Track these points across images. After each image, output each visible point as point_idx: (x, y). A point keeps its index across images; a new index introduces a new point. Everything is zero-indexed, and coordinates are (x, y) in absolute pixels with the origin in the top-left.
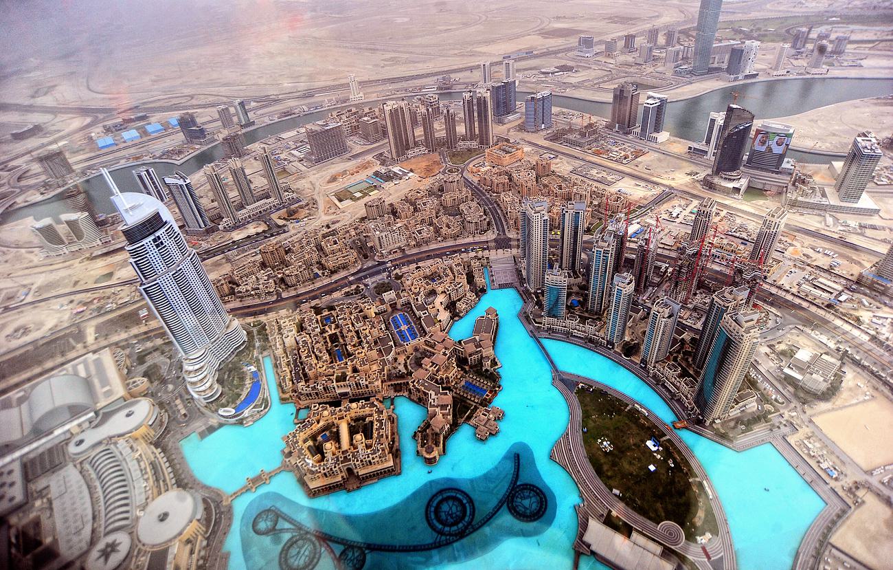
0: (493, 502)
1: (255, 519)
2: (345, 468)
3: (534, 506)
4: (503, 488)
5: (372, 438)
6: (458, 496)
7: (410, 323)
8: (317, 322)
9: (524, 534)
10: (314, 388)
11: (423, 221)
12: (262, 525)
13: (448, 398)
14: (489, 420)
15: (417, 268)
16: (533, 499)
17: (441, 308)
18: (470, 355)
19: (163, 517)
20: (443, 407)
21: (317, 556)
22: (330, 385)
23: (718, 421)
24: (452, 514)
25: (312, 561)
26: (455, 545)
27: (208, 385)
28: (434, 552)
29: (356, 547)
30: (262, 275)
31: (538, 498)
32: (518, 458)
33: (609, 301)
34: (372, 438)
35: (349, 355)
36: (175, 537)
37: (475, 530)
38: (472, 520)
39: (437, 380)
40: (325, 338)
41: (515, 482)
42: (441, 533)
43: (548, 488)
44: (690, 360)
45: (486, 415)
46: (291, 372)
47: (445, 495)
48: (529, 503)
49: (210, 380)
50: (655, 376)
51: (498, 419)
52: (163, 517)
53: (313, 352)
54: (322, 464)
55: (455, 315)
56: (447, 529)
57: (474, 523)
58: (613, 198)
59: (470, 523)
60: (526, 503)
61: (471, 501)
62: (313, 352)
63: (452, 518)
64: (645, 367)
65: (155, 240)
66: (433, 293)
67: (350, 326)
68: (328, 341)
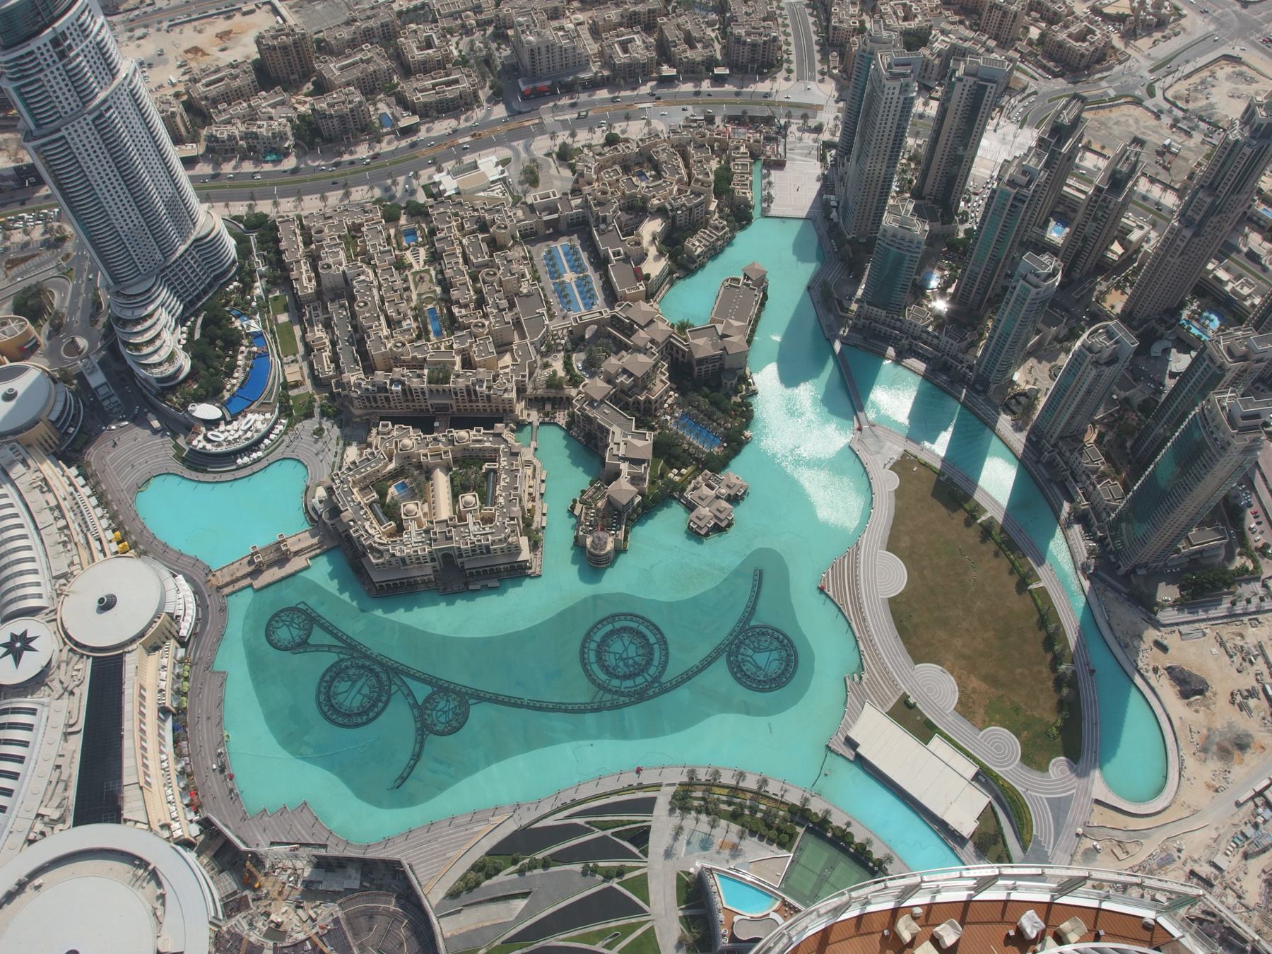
0: (704, 650)
1: (269, 624)
2: (440, 554)
3: (775, 665)
4: (729, 624)
5: (494, 504)
6: (642, 629)
7: (584, 270)
8: (388, 239)
9: (748, 710)
10: (382, 389)
11: (631, 20)
12: (284, 634)
13: (644, 445)
14: (718, 497)
15: (611, 140)
16: (775, 655)
17: (653, 251)
18: (701, 361)
19: (106, 604)
20: (636, 462)
21: (384, 699)
22: (415, 383)
23: (1140, 572)
24: (628, 658)
25: (374, 705)
26: (626, 710)
27: (164, 354)
28: (590, 718)
29: (454, 691)
30: (264, 101)
31: (784, 654)
32: (761, 575)
33: (1005, 289)
34: (494, 504)
35: (453, 324)
36: (132, 641)
37: (666, 691)
38: (661, 673)
39: (627, 403)
40: (405, 280)
41: (748, 619)
42: (601, 687)
43: (803, 638)
44: (1129, 444)
45: (712, 488)
46: (334, 344)
47: (618, 625)
48: (766, 661)
49: (168, 343)
50: (1051, 465)
51: (734, 500)
52: (106, 604)
53: (385, 312)
54: (398, 539)
55: (683, 266)
56: (615, 682)
57: (663, 680)
58: (1074, 29)
59: (656, 679)
60: (761, 659)
61: (663, 641)
62: (382, 310)
63: (626, 665)
64: (1038, 442)
65: (56, 42)
66: (637, 210)
67: (461, 261)
68: (412, 287)
